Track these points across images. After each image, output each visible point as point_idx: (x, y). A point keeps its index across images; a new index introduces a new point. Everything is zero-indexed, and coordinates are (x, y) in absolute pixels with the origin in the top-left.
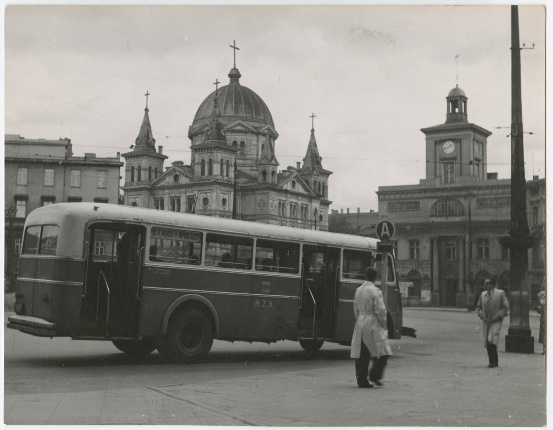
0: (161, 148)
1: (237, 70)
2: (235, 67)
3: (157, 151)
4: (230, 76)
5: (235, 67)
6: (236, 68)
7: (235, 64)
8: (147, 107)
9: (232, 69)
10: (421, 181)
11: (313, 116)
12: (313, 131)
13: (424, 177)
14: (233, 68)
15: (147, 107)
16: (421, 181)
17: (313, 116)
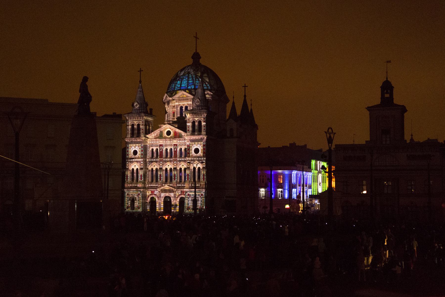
0: (151, 110)
1: (198, 53)
2: (196, 51)
3: (149, 112)
4: (192, 57)
5: (196, 51)
6: (198, 51)
7: (196, 49)
8: (140, 80)
9: (194, 53)
10: (366, 141)
11: (245, 86)
12: (245, 96)
13: (368, 139)
14: (195, 51)
15: (140, 80)
16: (366, 141)
17: (245, 86)
